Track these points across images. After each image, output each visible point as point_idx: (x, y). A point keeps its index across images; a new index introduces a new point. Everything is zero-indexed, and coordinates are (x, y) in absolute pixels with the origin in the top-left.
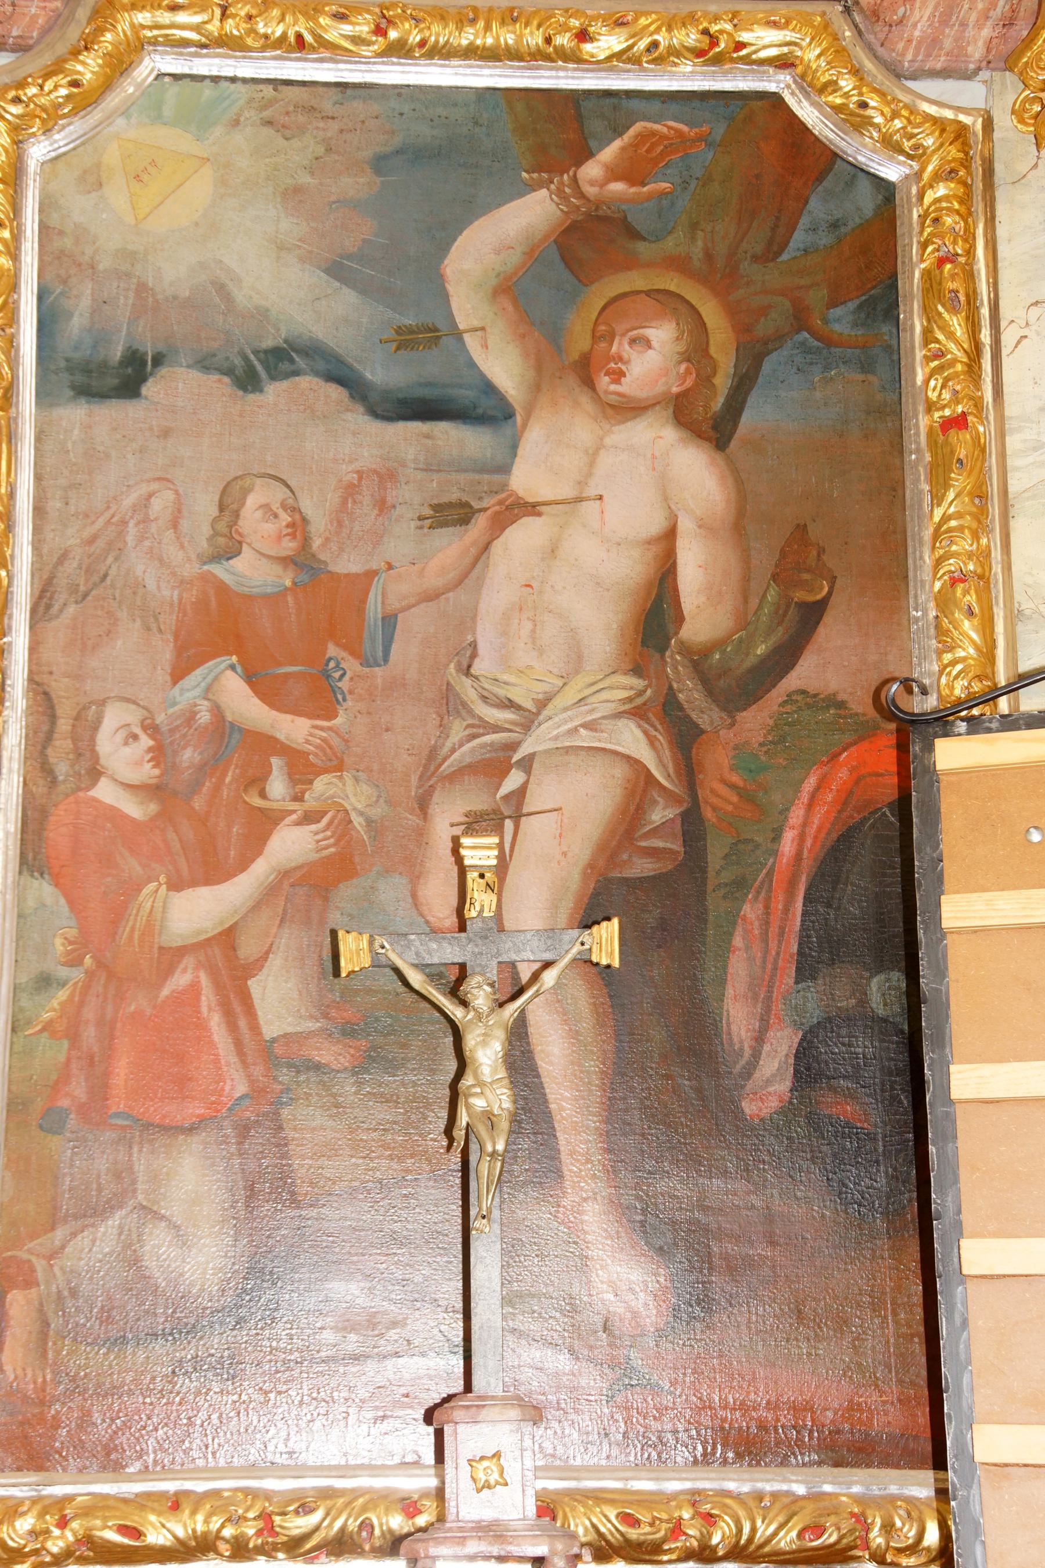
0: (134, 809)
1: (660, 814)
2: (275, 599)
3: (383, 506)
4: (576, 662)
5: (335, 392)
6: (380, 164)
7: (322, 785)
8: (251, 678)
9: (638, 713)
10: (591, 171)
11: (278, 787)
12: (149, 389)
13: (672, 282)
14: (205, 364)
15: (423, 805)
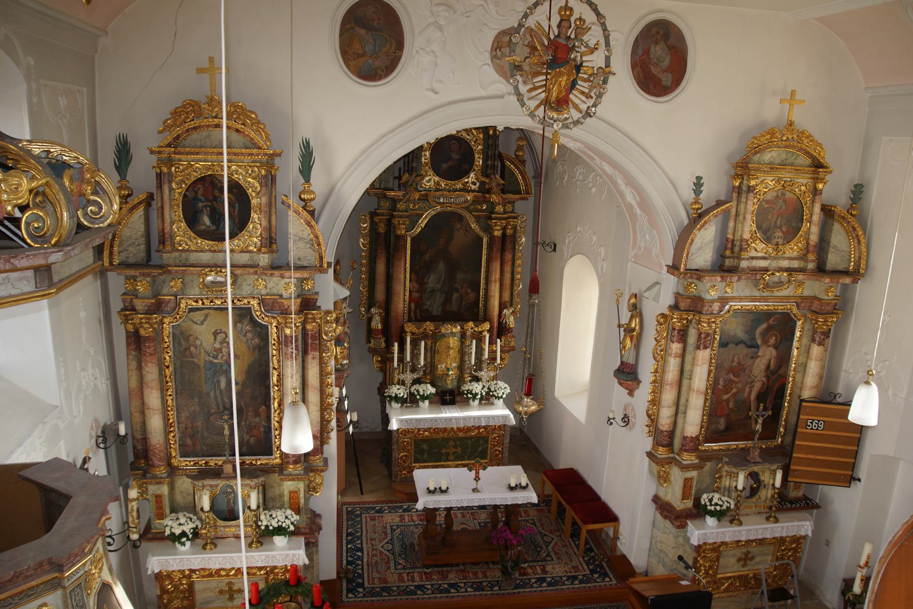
0: (721, 388)
1: (765, 386)
2: (736, 367)
3: (747, 357)
4: (761, 371)
5: (744, 345)
6: (752, 321)
7: (738, 385)
8: (733, 375)
9: (764, 376)
10: (771, 321)
11: (734, 385)
12: (728, 346)
13: (775, 333)
14: (733, 343)
15: (746, 386)
